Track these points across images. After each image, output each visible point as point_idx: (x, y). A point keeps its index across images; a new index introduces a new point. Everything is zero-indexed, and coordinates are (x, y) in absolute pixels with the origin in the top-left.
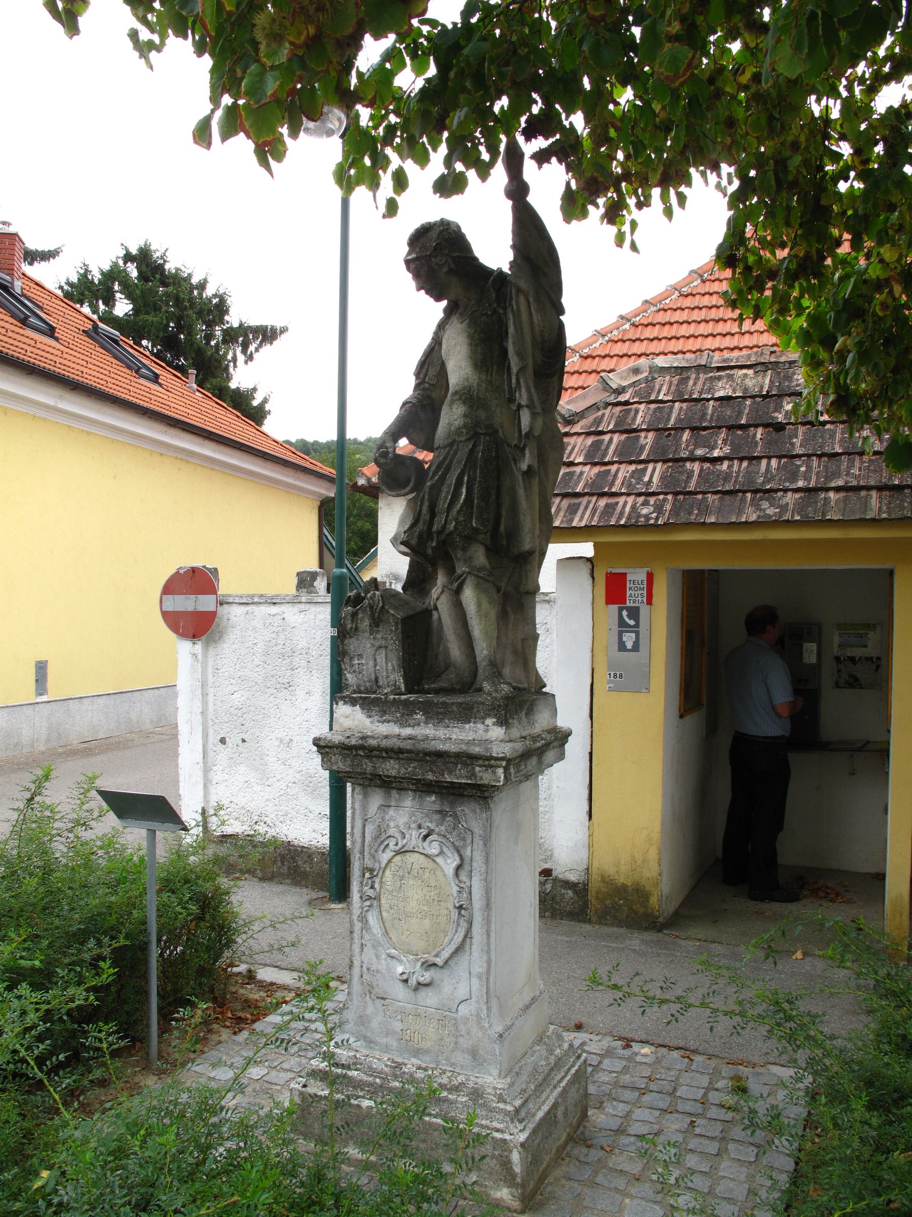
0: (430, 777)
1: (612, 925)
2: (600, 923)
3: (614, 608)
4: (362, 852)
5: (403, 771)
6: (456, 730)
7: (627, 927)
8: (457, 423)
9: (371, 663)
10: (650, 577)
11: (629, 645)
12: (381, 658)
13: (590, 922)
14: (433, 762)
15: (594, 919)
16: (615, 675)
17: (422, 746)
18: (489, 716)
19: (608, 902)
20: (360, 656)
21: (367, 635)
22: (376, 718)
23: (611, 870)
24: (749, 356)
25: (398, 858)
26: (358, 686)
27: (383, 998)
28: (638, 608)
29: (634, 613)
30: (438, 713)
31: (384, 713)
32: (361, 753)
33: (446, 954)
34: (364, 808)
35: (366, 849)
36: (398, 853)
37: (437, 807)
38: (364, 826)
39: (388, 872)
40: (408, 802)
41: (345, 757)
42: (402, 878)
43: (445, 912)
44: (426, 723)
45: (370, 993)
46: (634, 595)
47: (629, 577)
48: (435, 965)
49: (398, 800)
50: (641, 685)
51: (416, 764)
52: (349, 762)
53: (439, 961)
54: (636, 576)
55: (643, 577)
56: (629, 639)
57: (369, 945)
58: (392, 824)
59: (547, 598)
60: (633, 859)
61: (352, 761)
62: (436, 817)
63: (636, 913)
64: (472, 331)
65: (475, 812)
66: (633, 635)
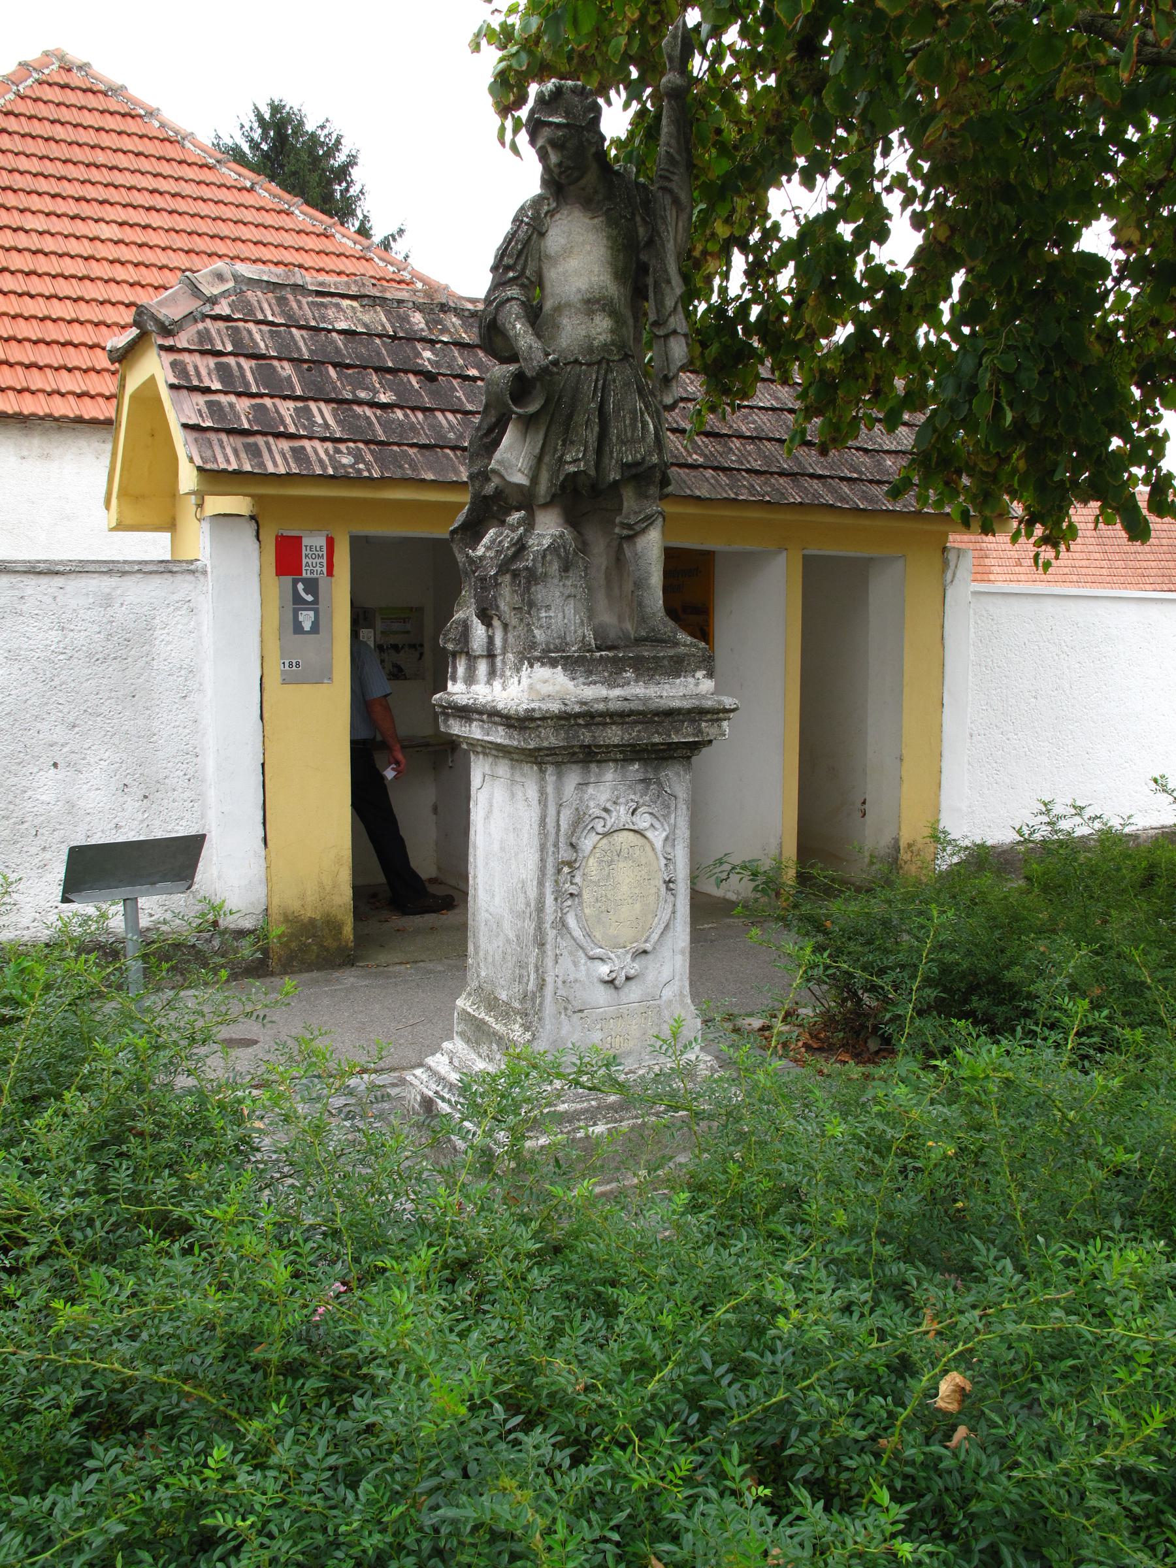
0: (657, 739)
1: (301, 971)
2: (286, 973)
3: (288, 579)
4: (556, 845)
5: (626, 737)
6: (667, 686)
7: (319, 969)
8: (602, 338)
9: (560, 615)
10: (330, 542)
11: (307, 626)
12: (570, 609)
13: (272, 974)
14: (660, 723)
15: (277, 970)
16: (291, 664)
17: (652, 706)
18: (699, 668)
19: (293, 945)
20: (548, 608)
21: (556, 581)
22: (581, 680)
23: (295, 905)
24: (347, 284)
25: (605, 841)
26: (547, 644)
27: (581, 1011)
28: (316, 580)
29: (312, 586)
30: (649, 669)
31: (590, 673)
32: (581, 721)
33: (655, 936)
34: (559, 790)
35: (562, 839)
36: (605, 835)
37: (640, 776)
38: (558, 813)
39: (591, 861)
40: (610, 775)
41: (557, 728)
42: (610, 863)
43: (654, 890)
44: (637, 681)
45: (566, 1009)
46: (312, 565)
47: (305, 542)
48: (645, 952)
49: (599, 775)
50: (323, 675)
51: (640, 727)
52: (562, 734)
53: (648, 947)
54: (313, 542)
55: (321, 541)
56: (307, 619)
57: (565, 953)
58: (592, 804)
59: (192, 567)
60: (321, 885)
61: (567, 732)
62: (640, 787)
63: (327, 949)
64: (615, 232)
65: (678, 774)
66: (312, 613)
